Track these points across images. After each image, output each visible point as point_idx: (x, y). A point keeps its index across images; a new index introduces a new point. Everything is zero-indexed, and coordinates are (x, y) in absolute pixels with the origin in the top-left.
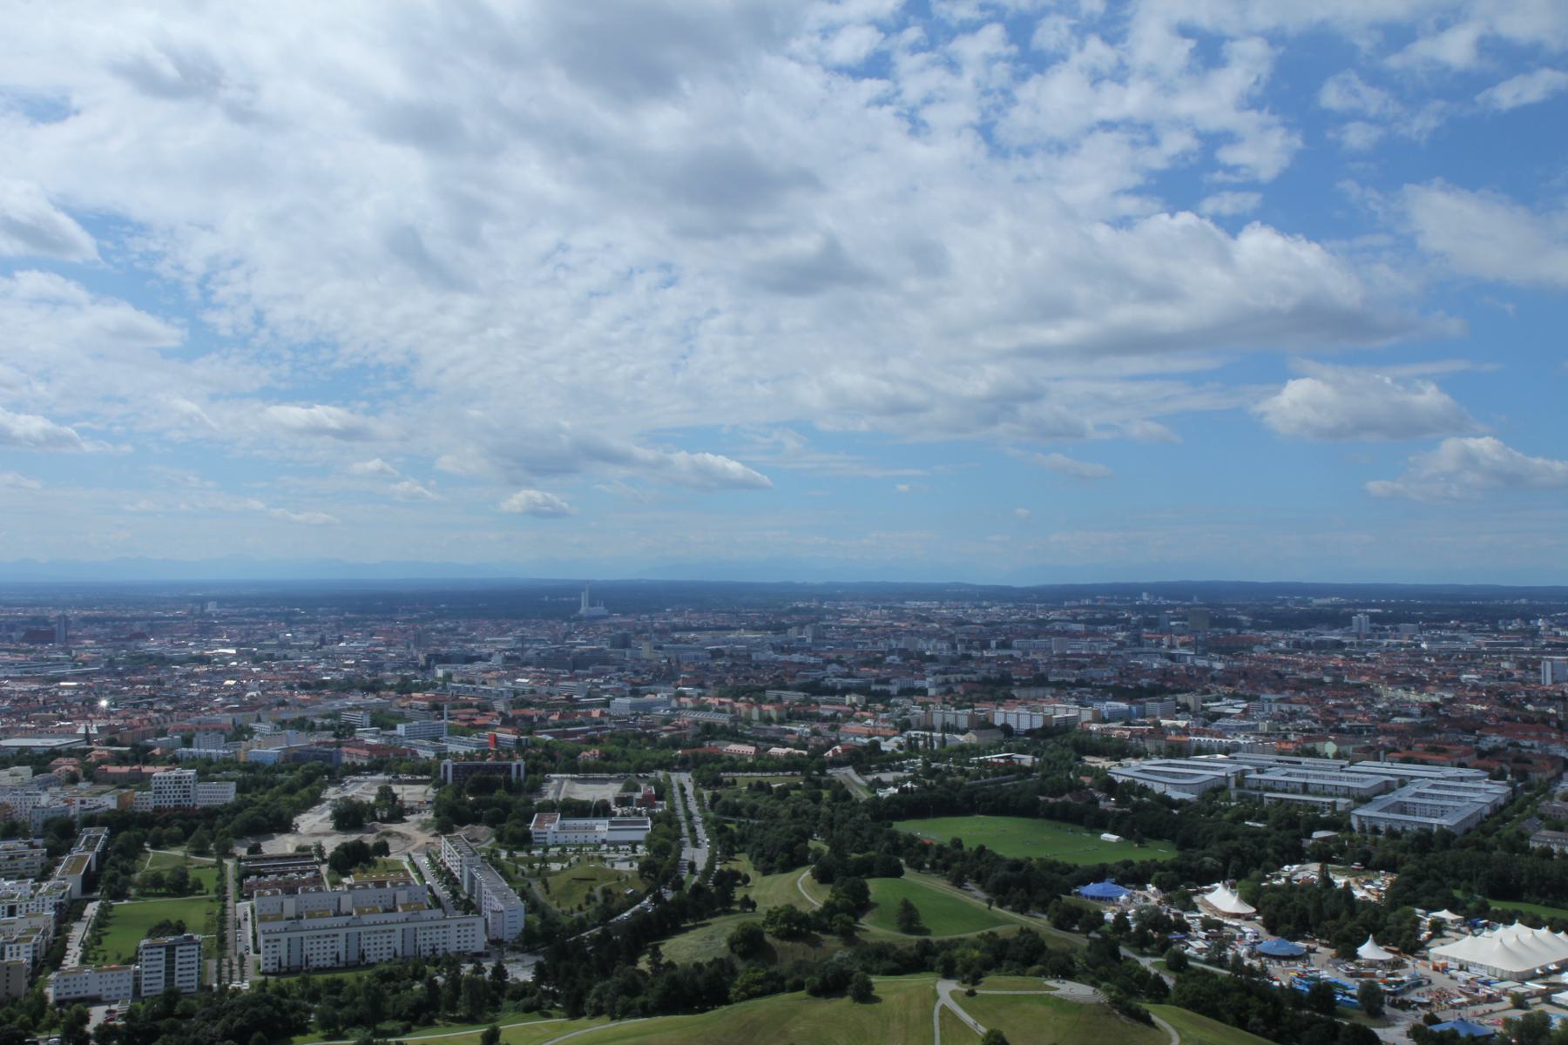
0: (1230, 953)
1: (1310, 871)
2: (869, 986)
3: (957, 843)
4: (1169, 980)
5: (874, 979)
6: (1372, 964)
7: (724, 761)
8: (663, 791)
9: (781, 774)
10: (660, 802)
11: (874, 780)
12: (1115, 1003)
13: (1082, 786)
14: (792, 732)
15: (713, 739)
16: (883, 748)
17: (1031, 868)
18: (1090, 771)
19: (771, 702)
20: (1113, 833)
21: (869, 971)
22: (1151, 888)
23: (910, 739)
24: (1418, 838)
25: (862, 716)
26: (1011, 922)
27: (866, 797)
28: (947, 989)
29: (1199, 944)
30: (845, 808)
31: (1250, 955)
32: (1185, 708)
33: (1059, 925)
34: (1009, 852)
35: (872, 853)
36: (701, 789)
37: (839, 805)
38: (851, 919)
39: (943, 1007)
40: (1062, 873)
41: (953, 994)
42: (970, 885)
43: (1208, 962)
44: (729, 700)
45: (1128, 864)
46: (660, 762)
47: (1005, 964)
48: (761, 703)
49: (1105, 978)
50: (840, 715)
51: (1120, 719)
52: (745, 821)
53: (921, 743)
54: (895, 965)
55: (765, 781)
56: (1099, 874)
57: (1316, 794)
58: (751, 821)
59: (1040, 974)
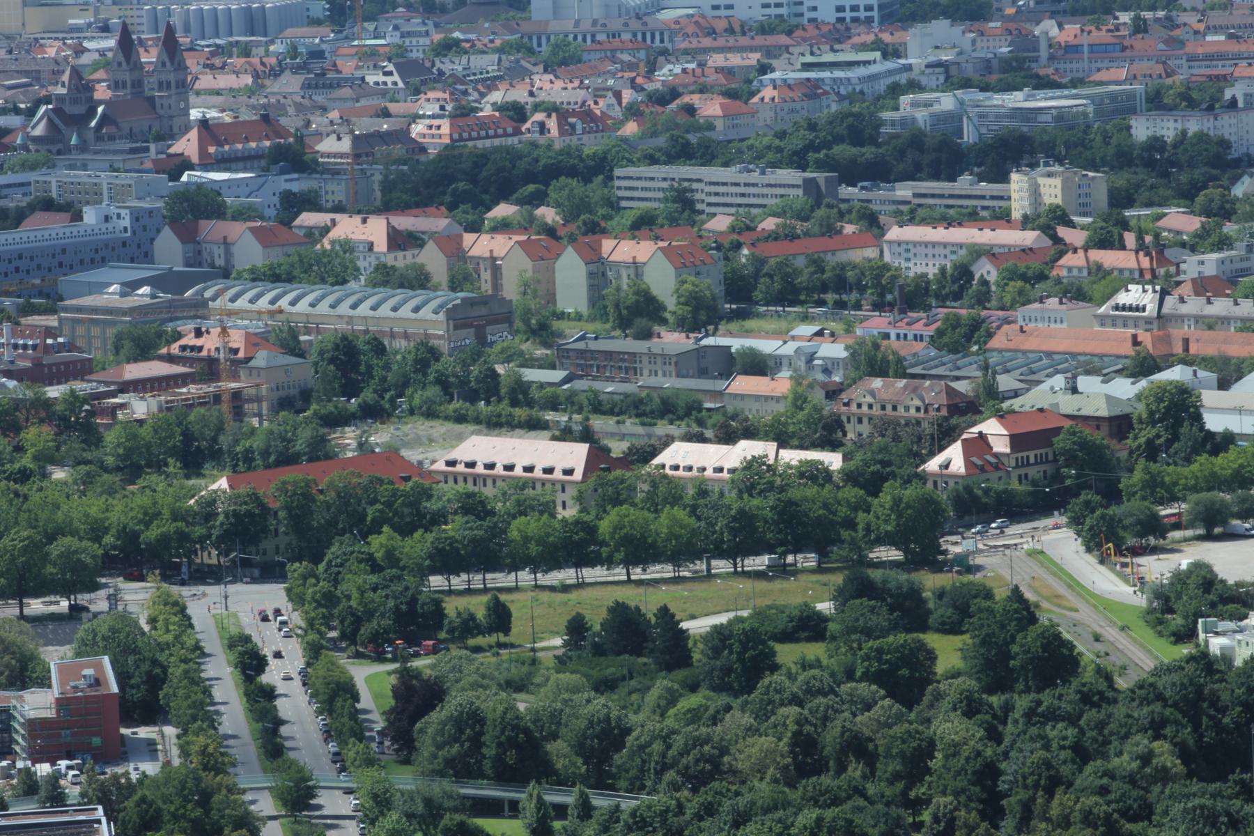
7: (439, 518)
8: (156, 680)
9: (721, 566)
10: (144, 732)
11: (1180, 578)
14: (758, 365)
15: (374, 413)
16: (1214, 423)
19: (643, 225)
25: (1099, 271)
27: (1149, 664)
30: (1052, 716)
36: (343, 660)
37: (1022, 703)
44: (435, 222)
46: (129, 538)
48: (595, 229)
50: (986, 270)
52: (568, 799)
55: (649, 603)
58: (601, 802)
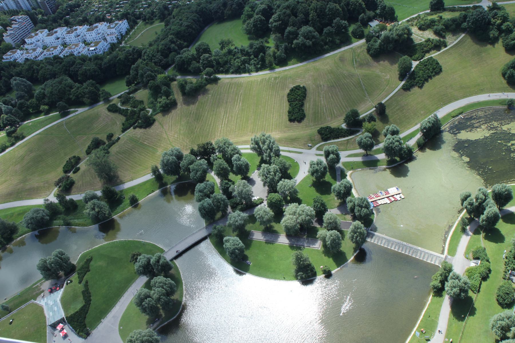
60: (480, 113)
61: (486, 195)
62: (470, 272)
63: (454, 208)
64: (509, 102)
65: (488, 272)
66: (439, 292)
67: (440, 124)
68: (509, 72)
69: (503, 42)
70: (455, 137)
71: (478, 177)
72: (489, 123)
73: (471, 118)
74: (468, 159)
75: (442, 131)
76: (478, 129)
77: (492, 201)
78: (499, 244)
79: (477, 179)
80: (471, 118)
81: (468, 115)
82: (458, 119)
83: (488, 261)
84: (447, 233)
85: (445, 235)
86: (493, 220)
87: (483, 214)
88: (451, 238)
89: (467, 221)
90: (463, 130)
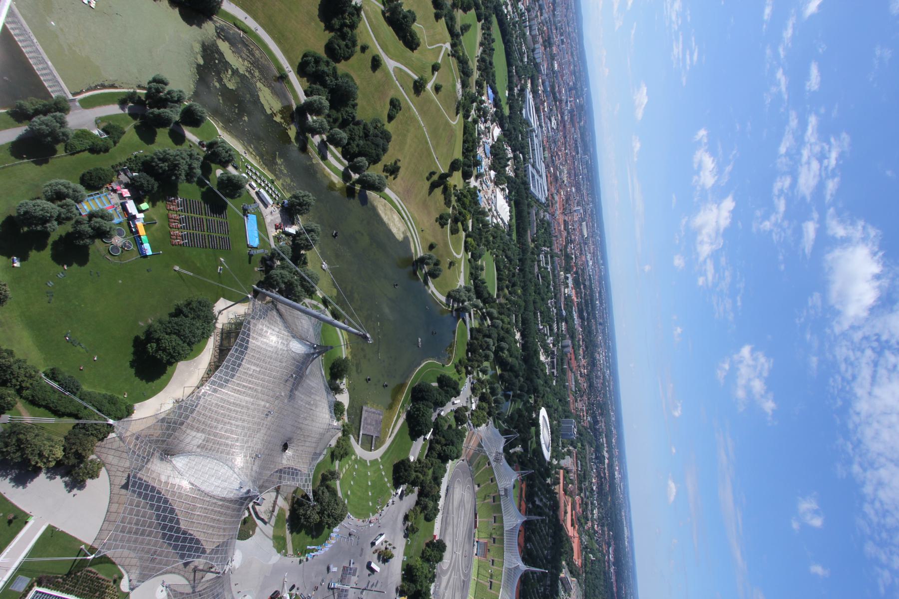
0: (482, 136)
1: (510, 155)
2: (441, 18)
3: (493, 41)
4: (470, 119)
5: (443, 19)
6: (490, 175)
12: (459, 103)
13: (521, 81)
17: (491, 69)
18: (526, 82)
20: (509, 94)
21: (445, 16)
22: (495, 109)
23: (524, 13)
24: (526, 182)
26: (474, 65)
28: (448, 46)
29: (483, 127)
31: (483, 142)
32: (551, 110)
33: (477, 82)
34: (495, 60)
35: (483, 8)
38: (460, 6)
39: (442, 46)
40: (492, 80)
41: (447, 49)
42: (481, 48)
43: (478, 130)
45: (500, 100)
47: (461, 64)
49: (465, 99)
51: (544, 89)
53: (524, 18)
54: (450, 25)
56: (495, 92)
57: (532, 153)
59: (461, 77)
60: (257, 52)
61: (179, 100)
62: (83, 134)
63: (137, 78)
64: (284, 74)
65: (103, 149)
66: (19, 115)
67: (217, 12)
68: (310, 58)
69: (332, 37)
70: (215, 38)
71: (192, 86)
72: (254, 66)
73: (246, 46)
74: (201, 62)
75: (211, 19)
76: (240, 60)
77: (180, 110)
78: (142, 142)
79: (189, 87)
80: (246, 46)
81: (247, 41)
82: (237, 32)
83: (115, 143)
84: (103, 86)
85: (99, 85)
86: (163, 122)
87: (159, 109)
88: (101, 94)
89: (137, 98)
90: (230, 43)
